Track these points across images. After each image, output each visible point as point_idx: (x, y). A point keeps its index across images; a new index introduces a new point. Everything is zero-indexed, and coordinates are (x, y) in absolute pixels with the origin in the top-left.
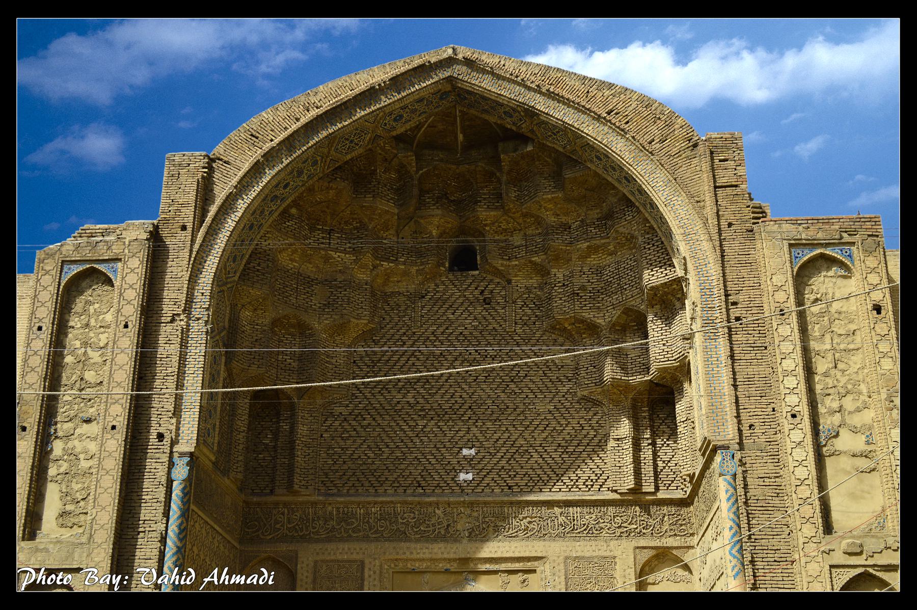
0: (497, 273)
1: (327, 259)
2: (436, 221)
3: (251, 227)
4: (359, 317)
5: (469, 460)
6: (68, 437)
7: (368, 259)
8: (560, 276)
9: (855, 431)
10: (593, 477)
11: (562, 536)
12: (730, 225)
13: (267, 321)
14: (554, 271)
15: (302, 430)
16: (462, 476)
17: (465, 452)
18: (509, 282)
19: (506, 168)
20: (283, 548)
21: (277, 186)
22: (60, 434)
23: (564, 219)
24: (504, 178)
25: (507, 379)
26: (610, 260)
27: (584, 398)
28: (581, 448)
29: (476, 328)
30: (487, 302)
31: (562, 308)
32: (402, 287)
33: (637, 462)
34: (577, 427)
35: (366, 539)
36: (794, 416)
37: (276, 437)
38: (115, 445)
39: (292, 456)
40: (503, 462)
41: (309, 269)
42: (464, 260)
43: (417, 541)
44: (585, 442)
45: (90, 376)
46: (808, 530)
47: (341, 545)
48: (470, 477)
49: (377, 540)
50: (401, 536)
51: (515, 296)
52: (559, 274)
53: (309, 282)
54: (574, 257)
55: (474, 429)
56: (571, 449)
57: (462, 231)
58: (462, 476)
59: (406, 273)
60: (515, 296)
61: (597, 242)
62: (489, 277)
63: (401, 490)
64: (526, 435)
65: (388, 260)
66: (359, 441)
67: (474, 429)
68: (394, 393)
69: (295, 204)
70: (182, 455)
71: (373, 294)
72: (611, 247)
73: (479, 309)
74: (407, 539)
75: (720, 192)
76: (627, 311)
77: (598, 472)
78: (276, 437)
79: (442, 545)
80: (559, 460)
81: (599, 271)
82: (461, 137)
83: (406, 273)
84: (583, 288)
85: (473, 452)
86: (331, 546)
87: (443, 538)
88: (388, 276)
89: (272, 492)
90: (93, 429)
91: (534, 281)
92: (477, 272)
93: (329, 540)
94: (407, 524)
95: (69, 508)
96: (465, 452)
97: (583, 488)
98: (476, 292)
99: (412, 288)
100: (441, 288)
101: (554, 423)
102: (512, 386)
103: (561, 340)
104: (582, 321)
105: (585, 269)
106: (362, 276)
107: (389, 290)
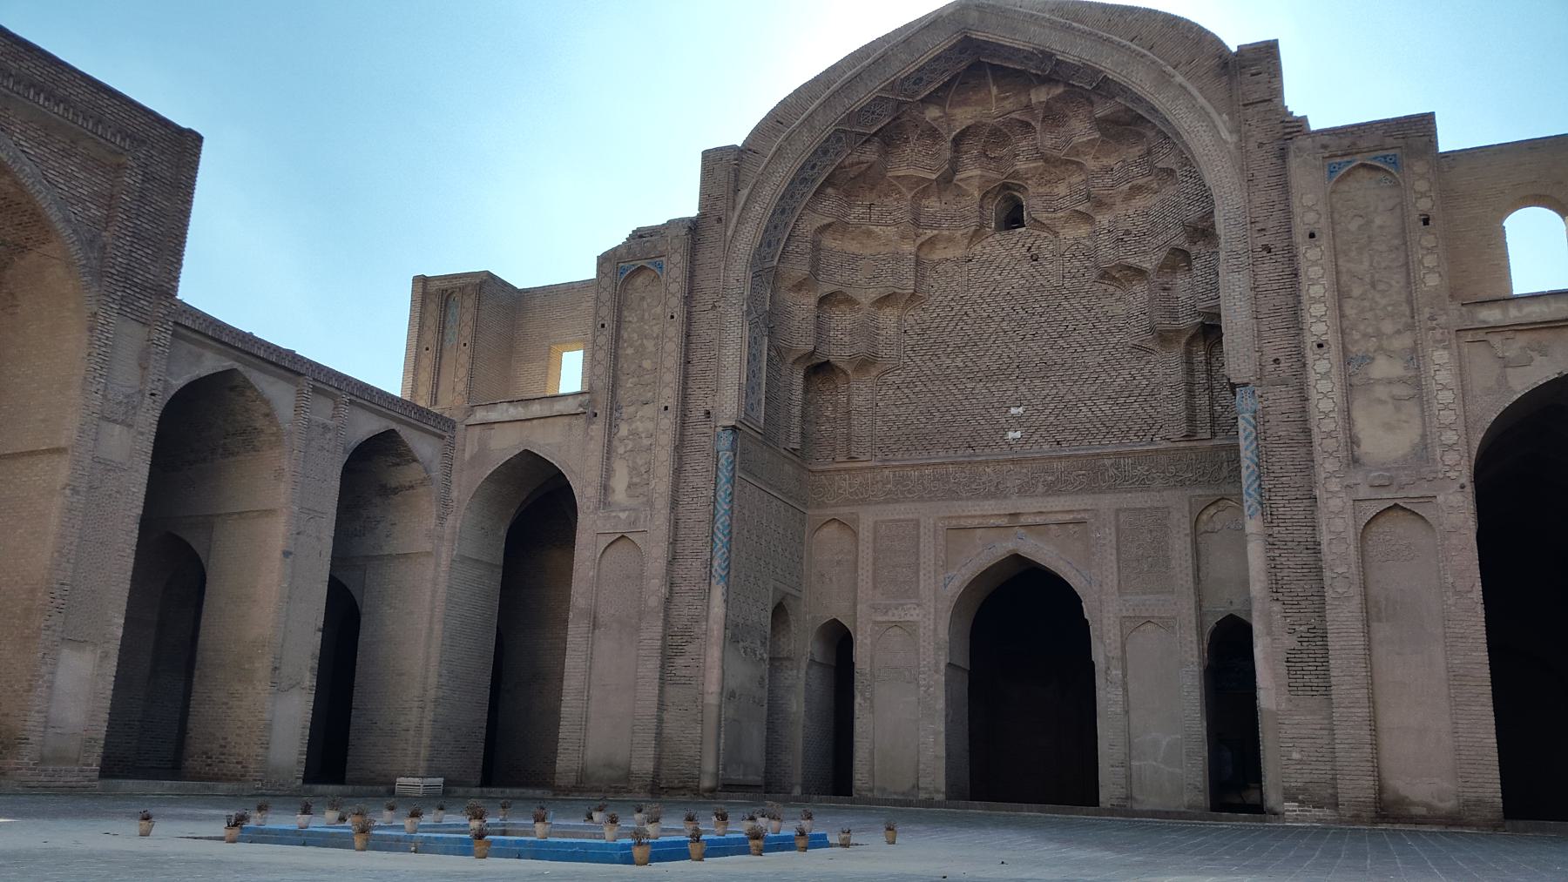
1: (869, 233)
3: (783, 212)
6: (630, 420)
8: (1105, 222)
9: (1390, 355)
10: (1145, 427)
11: (1112, 488)
12: (1261, 145)
14: (1098, 218)
15: (858, 401)
16: (1011, 435)
17: (1013, 411)
18: (1056, 234)
20: (846, 510)
21: (802, 168)
22: (625, 416)
23: (1105, 161)
25: (1055, 335)
26: (1155, 199)
28: (1132, 399)
31: (1108, 254)
32: (950, 253)
34: (1128, 377)
35: (921, 499)
36: (1320, 346)
38: (668, 422)
39: (849, 426)
40: (1052, 419)
41: (852, 247)
42: (1013, 218)
43: (968, 499)
44: (1136, 392)
45: (647, 364)
46: (1330, 465)
48: (1018, 435)
49: (931, 499)
51: (1063, 248)
52: (1103, 219)
53: (855, 257)
54: (1118, 200)
55: (1022, 388)
56: (1121, 400)
57: (1005, 187)
58: (1011, 435)
61: (1140, 181)
63: (951, 452)
64: (1075, 390)
65: (931, 227)
67: (1022, 388)
70: (725, 428)
72: (1155, 185)
75: (1250, 110)
76: (1176, 251)
77: (1150, 421)
79: (992, 502)
80: (1109, 412)
83: (950, 240)
84: (1127, 233)
85: (1021, 410)
87: (993, 496)
88: (931, 242)
90: (648, 411)
91: (1084, 230)
93: (887, 502)
94: (959, 484)
95: (636, 480)
96: (1013, 411)
97: (1135, 439)
98: (1024, 250)
100: (988, 250)
101: (1103, 376)
102: (1061, 342)
103: (1111, 289)
104: (1129, 268)
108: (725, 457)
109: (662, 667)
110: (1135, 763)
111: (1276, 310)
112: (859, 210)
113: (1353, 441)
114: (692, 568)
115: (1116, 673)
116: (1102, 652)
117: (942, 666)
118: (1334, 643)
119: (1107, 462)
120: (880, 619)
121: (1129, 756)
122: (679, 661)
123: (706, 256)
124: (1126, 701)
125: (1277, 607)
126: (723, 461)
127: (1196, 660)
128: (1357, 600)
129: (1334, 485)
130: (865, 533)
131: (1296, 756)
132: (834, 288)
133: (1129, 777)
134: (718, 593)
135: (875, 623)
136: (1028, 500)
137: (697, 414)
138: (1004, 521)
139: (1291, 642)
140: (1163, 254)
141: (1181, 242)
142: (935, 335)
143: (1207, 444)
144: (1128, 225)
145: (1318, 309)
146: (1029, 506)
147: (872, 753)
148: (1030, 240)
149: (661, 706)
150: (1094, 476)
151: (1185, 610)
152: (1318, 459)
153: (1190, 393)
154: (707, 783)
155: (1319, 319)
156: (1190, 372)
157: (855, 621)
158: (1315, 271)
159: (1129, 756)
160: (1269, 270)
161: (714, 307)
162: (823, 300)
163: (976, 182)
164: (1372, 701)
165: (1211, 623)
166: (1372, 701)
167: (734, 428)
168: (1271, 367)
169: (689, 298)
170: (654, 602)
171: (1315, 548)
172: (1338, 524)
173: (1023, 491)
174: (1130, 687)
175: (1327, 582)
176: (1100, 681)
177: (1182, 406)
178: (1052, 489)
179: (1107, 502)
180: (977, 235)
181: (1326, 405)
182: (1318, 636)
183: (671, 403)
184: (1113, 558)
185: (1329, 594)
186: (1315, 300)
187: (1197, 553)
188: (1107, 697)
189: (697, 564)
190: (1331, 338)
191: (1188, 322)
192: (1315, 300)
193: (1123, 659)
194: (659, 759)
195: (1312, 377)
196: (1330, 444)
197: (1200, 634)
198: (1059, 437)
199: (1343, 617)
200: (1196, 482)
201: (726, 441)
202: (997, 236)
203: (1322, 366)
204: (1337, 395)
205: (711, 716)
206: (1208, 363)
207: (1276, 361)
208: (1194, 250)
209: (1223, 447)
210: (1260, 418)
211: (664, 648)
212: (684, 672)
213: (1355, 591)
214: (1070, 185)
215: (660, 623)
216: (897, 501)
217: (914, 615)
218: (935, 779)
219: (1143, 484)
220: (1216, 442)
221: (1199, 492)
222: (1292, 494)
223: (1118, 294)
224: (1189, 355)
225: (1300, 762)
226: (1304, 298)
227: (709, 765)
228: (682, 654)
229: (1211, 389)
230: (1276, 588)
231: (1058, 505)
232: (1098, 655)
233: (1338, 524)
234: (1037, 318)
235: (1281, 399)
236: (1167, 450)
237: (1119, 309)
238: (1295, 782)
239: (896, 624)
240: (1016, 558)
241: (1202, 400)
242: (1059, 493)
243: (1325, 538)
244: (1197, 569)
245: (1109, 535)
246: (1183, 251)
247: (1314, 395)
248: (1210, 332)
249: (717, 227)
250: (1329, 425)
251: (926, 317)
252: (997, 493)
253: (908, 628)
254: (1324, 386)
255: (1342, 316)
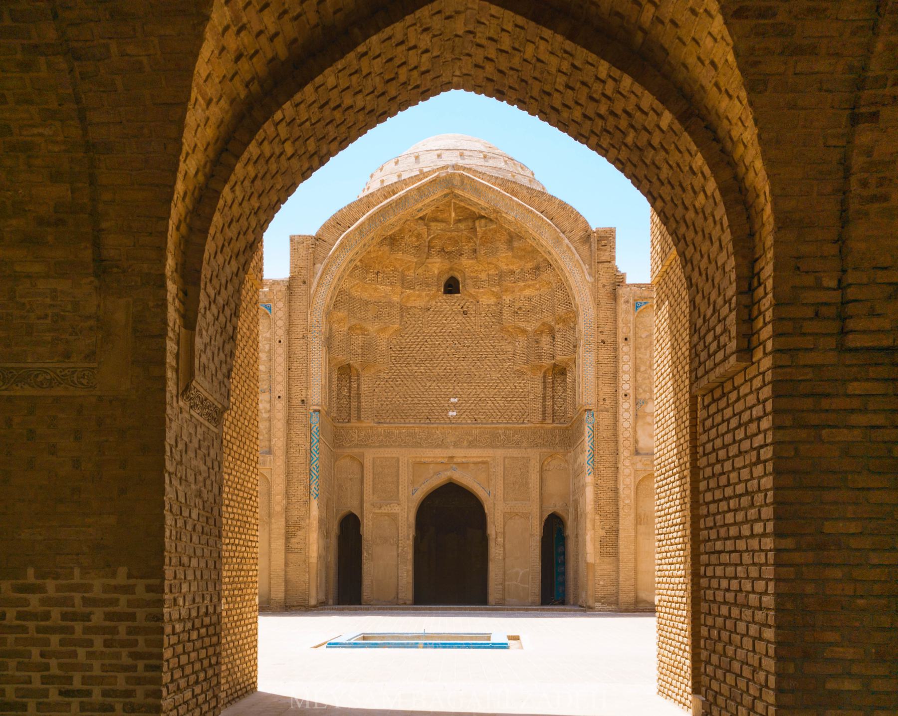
0: (471, 295)
1: (376, 290)
2: (437, 265)
4: (394, 323)
5: (455, 404)
7: (399, 290)
11: (503, 446)
13: (346, 329)
14: (504, 297)
16: (451, 413)
17: (452, 400)
19: (479, 236)
24: (478, 242)
27: (517, 370)
29: (458, 329)
30: (465, 313)
32: (418, 303)
33: (544, 406)
35: (400, 446)
37: (350, 391)
40: (473, 406)
41: (365, 296)
42: (452, 287)
47: (387, 449)
48: (455, 414)
49: (405, 446)
50: (418, 445)
52: (507, 298)
53: (367, 303)
54: (516, 290)
57: (451, 269)
58: (451, 413)
59: (419, 296)
60: (481, 309)
62: (466, 298)
65: (409, 288)
66: (395, 393)
67: (457, 388)
68: (413, 366)
69: (361, 261)
70: (315, 411)
71: (401, 308)
73: (461, 317)
74: (421, 447)
76: (543, 324)
78: (350, 391)
81: (530, 299)
82: (453, 215)
83: (419, 296)
84: (520, 309)
85: (456, 400)
86: (382, 450)
88: (408, 296)
89: (349, 421)
91: (493, 300)
92: (459, 295)
93: (380, 447)
96: (452, 400)
98: (459, 307)
99: (422, 304)
100: (439, 304)
102: (478, 363)
105: (522, 298)
106: (396, 299)
107: (409, 305)
108: (316, 426)
109: (286, 544)
110: (507, 583)
111: (606, 373)
112: (371, 276)
113: (636, 442)
114: (299, 490)
115: (500, 540)
116: (493, 529)
117: (411, 537)
118: (622, 534)
119: (500, 431)
120: (377, 511)
121: (504, 580)
122: (293, 540)
123: (299, 305)
124: (504, 553)
125: (598, 517)
126: (314, 429)
127: (538, 533)
128: (633, 515)
129: (627, 463)
130: (368, 463)
131: (601, 583)
132: (357, 321)
133: (504, 590)
134: (315, 504)
135: (374, 513)
136: (459, 450)
137: (296, 401)
138: (446, 460)
139: (602, 533)
140: (538, 324)
141: (550, 320)
142: (408, 352)
143: (550, 426)
144: (521, 304)
145: (626, 377)
146: (460, 454)
147: (372, 582)
148: (463, 302)
149: (286, 565)
150: (494, 440)
151: (535, 509)
152: (621, 450)
153: (544, 398)
154: (313, 602)
155: (626, 382)
156: (545, 388)
157: (362, 512)
158: (626, 358)
159: (504, 580)
160: (605, 353)
161: (304, 337)
162: (350, 328)
163: (437, 265)
164: (636, 560)
165: (546, 516)
166: (636, 560)
167: (319, 411)
168: (601, 402)
169: (289, 332)
170: (278, 508)
171: (616, 490)
172: (628, 481)
173: (456, 445)
174: (506, 546)
175: (621, 506)
176: (492, 546)
177: (540, 405)
178: (471, 445)
179: (500, 453)
180: (435, 297)
181: (626, 425)
182: (615, 530)
183: (283, 394)
184: (502, 482)
185: (621, 513)
186: (625, 372)
187: (542, 480)
188: (495, 551)
189: (301, 487)
190: (631, 392)
191: (547, 362)
192: (625, 372)
193: (504, 533)
194: (286, 591)
195: (621, 410)
196: (627, 443)
197: (541, 520)
198: (476, 417)
199: (626, 523)
200: (543, 445)
201: (315, 420)
202: (444, 296)
203: (626, 405)
204: (631, 420)
205: (314, 571)
206: (553, 383)
207: (604, 399)
208: (557, 327)
209: (557, 428)
210: (595, 429)
211: (287, 532)
212: (297, 546)
213: (633, 511)
214: (488, 275)
215: (284, 520)
216: (387, 446)
217: (396, 509)
218: (408, 592)
219: (518, 445)
220: (555, 425)
221: (544, 450)
222: (607, 465)
223: (510, 339)
224: (544, 377)
225: (603, 586)
226: (621, 371)
227: (313, 593)
228: (295, 536)
229: (553, 397)
230: (598, 508)
231: (475, 454)
232: (491, 530)
233: (628, 481)
234: (466, 348)
235: (605, 418)
236: (530, 428)
237: (510, 348)
238: (600, 594)
239: (388, 515)
240: (451, 479)
241: (549, 403)
242: (475, 447)
243: (621, 487)
244: (541, 489)
245: (500, 470)
246: (551, 326)
247: (621, 420)
248: (560, 372)
249: (304, 287)
250: (627, 434)
251: (403, 340)
252: (442, 445)
253: (394, 518)
254: (626, 415)
255: (636, 380)
